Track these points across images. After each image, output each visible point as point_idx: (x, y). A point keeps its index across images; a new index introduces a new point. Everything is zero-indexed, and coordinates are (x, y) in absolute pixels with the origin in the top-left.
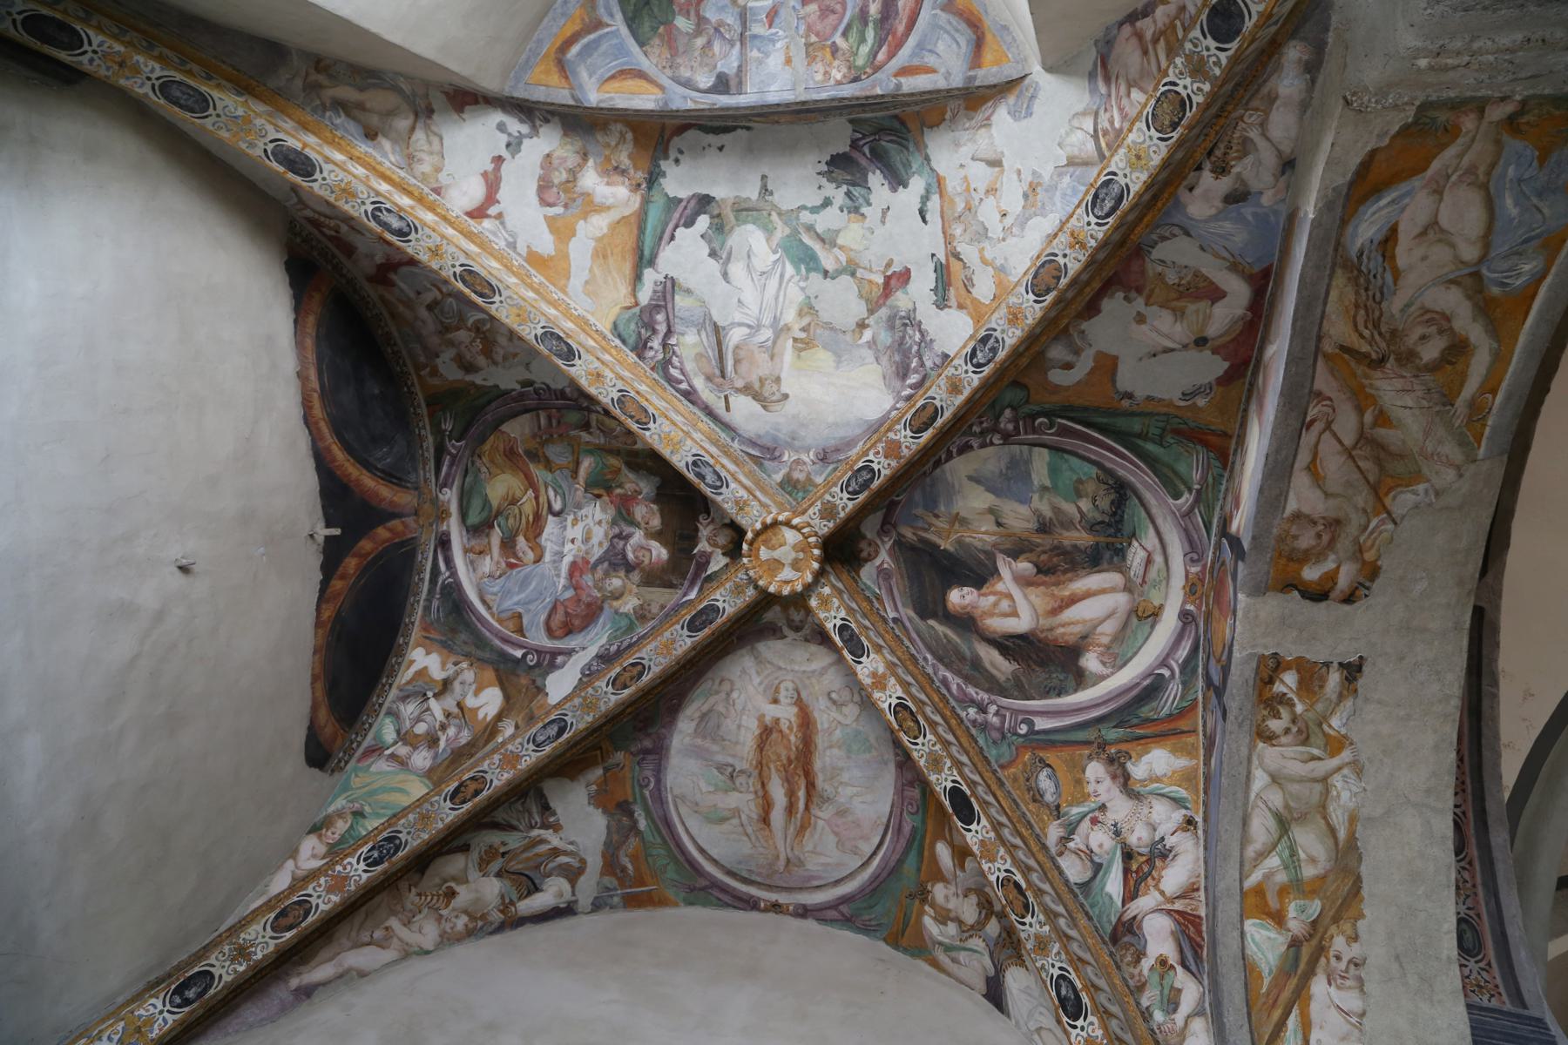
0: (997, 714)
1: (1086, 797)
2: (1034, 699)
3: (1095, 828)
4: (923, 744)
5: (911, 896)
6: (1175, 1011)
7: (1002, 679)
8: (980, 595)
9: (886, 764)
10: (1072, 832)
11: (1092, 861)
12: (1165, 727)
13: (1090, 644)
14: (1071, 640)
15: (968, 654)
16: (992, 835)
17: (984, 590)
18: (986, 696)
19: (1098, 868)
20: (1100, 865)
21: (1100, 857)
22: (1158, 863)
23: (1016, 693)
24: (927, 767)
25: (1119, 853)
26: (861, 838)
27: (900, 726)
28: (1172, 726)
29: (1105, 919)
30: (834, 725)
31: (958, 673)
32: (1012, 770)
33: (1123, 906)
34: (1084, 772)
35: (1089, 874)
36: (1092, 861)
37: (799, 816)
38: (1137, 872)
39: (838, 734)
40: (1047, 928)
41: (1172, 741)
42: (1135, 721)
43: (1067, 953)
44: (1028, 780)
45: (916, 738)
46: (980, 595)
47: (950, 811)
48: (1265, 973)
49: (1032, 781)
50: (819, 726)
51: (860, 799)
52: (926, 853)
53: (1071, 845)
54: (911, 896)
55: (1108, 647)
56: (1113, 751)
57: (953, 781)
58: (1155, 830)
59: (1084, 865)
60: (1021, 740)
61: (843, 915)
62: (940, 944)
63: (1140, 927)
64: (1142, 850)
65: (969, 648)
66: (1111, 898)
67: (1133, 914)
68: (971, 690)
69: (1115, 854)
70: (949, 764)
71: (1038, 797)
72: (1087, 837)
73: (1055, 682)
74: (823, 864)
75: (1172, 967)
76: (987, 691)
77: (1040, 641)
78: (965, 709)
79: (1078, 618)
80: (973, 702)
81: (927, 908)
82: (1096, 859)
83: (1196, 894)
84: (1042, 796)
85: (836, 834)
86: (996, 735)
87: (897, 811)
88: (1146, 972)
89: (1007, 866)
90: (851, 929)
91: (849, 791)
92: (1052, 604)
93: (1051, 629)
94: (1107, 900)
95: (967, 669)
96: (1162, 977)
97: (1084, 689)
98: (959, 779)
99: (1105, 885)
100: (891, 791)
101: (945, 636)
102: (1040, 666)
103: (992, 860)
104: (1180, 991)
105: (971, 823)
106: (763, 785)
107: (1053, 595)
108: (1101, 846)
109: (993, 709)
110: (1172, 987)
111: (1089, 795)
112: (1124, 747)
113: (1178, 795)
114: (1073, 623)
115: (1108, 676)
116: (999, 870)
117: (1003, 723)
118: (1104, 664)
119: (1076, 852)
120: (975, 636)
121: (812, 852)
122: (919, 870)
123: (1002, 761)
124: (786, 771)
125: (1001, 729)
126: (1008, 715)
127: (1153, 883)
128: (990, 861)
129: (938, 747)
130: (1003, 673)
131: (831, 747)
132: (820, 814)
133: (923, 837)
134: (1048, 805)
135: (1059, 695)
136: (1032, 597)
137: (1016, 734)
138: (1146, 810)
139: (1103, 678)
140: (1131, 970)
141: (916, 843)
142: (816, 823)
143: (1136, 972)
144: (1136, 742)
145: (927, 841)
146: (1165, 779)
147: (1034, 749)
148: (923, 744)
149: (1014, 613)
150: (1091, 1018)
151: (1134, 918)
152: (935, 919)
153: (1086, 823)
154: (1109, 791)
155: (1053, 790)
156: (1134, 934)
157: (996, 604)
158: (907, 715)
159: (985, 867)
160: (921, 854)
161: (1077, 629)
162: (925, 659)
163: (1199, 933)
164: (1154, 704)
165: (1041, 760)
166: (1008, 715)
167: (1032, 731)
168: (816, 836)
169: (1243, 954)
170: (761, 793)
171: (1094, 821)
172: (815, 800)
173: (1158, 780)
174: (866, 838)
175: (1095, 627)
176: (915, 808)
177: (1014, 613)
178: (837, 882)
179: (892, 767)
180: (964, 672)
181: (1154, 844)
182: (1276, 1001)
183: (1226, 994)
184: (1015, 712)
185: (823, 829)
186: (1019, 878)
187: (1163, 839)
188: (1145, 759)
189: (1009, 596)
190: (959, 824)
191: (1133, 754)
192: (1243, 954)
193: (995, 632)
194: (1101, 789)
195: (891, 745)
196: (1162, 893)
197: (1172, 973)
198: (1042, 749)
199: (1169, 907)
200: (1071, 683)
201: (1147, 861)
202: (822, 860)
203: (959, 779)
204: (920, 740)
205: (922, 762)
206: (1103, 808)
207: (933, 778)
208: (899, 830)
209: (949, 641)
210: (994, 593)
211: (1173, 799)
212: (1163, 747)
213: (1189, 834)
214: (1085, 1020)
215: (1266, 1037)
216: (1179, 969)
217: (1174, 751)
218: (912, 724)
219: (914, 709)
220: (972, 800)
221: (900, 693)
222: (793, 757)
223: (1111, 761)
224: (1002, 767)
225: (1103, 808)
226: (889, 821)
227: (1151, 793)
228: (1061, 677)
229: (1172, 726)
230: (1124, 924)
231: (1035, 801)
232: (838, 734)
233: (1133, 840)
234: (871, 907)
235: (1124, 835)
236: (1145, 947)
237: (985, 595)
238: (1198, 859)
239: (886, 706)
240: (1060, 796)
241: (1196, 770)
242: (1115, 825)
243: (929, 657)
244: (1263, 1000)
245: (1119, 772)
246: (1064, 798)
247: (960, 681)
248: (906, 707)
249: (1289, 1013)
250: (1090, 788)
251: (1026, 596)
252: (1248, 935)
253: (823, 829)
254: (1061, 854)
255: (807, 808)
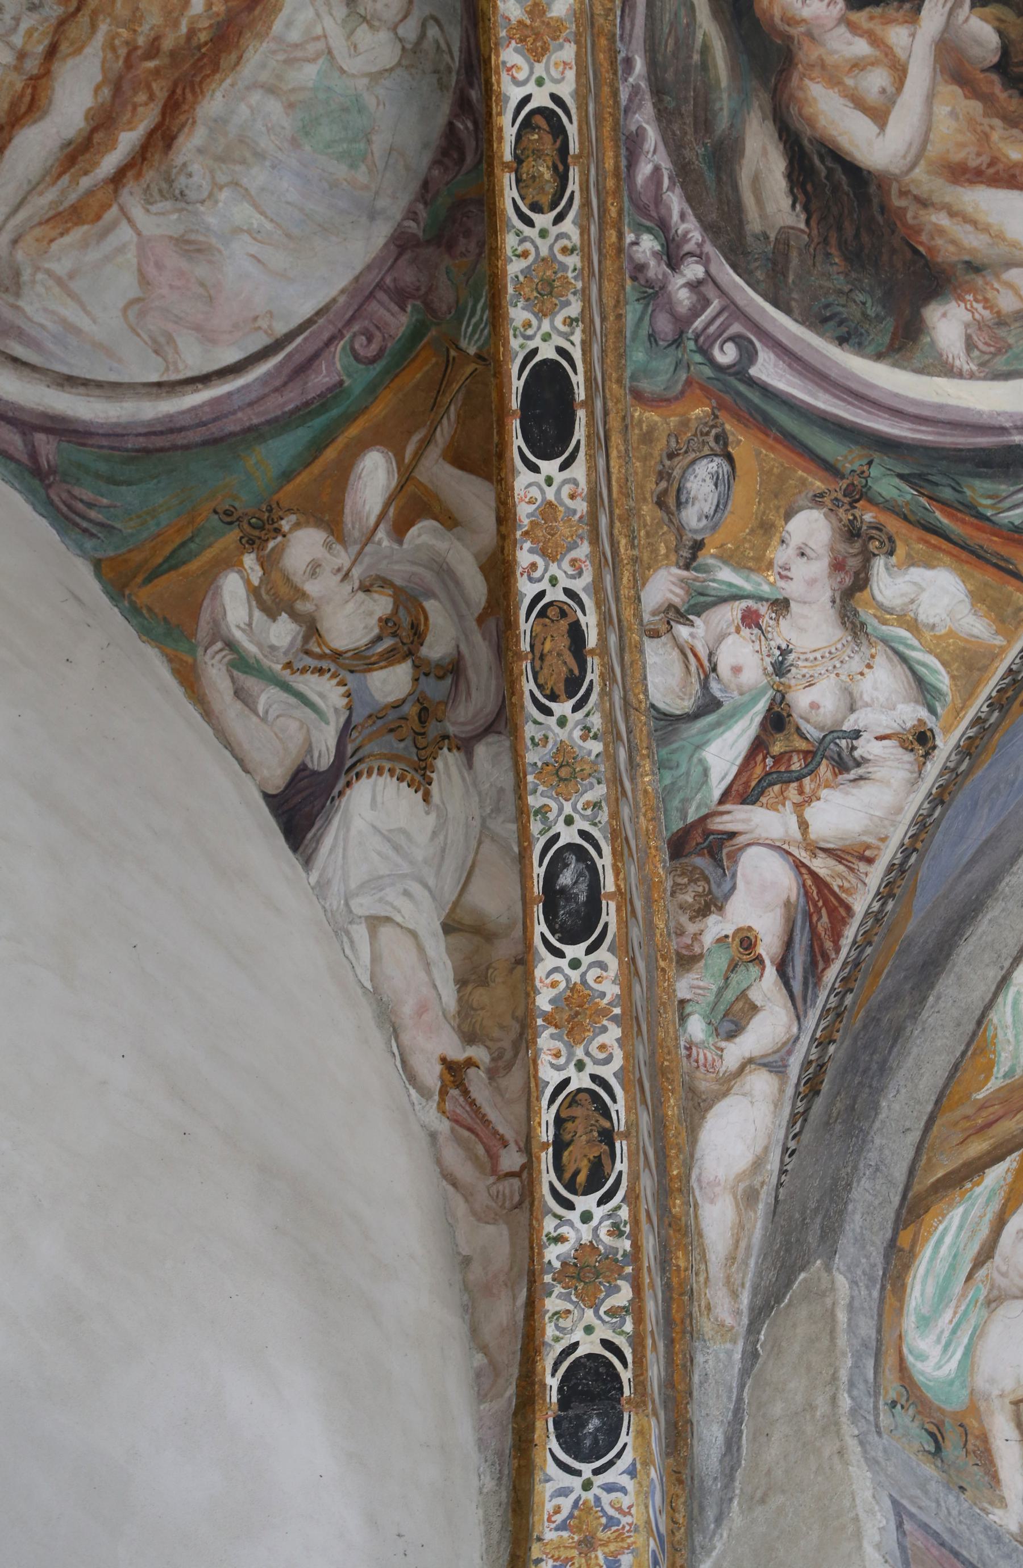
0: (695, 286)
1: (761, 564)
2: (788, 311)
3: (745, 632)
4: (543, 234)
5: (229, 517)
6: (731, 1036)
7: (754, 223)
8: (843, 20)
9: (373, 215)
10: (699, 610)
11: (705, 685)
12: (993, 544)
13: (974, 290)
14: (946, 253)
15: (723, 122)
16: (581, 507)
17: (861, 17)
18: (696, 235)
19: (708, 705)
20: (717, 704)
21: (725, 689)
22: (824, 769)
23: (760, 275)
24: (519, 286)
25: (761, 706)
26: (198, 328)
27: (519, 160)
28: (1006, 551)
29: (676, 803)
30: (312, 48)
31: (674, 146)
32: (652, 416)
33: (724, 799)
34: (788, 516)
35: (684, 705)
36: (705, 685)
37: (86, 182)
38: (777, 759)
39: (309, 73)
40: (596, 747)
41: (988, 576)
42: (947, 493)
43: (615, 815)
44: (671, 456)
45: (536, 208)
46: (843, 20)
47: (515, 404)
48: (1001, 1070)
49: (680, 462)
50: (278, 26)
51: (254, 248)
52: (330, 454)
53: (683, 631)
54: (229, 517)
55: (1001, 321)
56: (868, 517)
57: (561, 351)
58: (852, 710)
59: (685, 684)
60: (708, 371)
61: (33, 455)
62: (231, 645)
63: (734, 857)
64: (805, 727)
65: (734, 114)
66: (706, 772)
67: (730, 827)
68: (675, 202)
69: (754, 700)
70: (574, 309)
71: (671, 502)
72: (722, 637)
73: (852, 312)
74: (64, 322)
75: (759, 960)
76: (709, 228)
77: (883, 209)
78: (639, 229)
79: (992, 219)
80: (662, 227)
81: (249, 560)
82: (715, 687)
83: (862, 867)
84: (679, 504)
85: (144, 280)
86: (664, 325)
87: (324, 329)
88: (708, 939)
89: (578, 585)
90: (29, 494)
91: (242, 213)
92: (969, 155)
93: (924, 203)
94: (696, 772)
95: (696, 153)
96: (733, 967)
97: (895, 365)
98: (577, 354)
99: (707, 742)
100: (342, 280)
101: (706, 49)
102: (846, 259)
103: (549, 554)
104: (754, 1009)
105: (548, 457)
106: (52, 52)
107: (985, 138)
108: (737, 670)
109: (694, 270)
110: (743, 995)
111: (770, 565)
112: (893, 525)
113: (930, 678)
114: (974, 223)
115: (960, 375)
116: (553, 581)
117: (695, 313)
118: (970, 345)
119: (685, 651)
120: (765, 97)
121: (59, 281)
122: (287, 476)
123: (645, 385)
124: (129, 65)
125: (682, 323)
126: (715, 305)
127: (797, 799)
128: (543, 553)
129: (573, 261)
130: (763, 216)
131: (271, 90)
132: (137, 212)
133: (349, 418)
134: (680, 530)
135: (842, 341)
136: (942, 111)
137: (705, 352)
138: (856, 664)
139: (948, 370)
140: (684, 919)
141: (319, 422)
142: (114, 225)
143: (692, 928)
144: (917, 533)
145: (353, 431)
146: (928, 635)
147: (721, 406)
148: (543, 234)
149: (879, 116)
150: (602, 954)
151: (732, 835)
152: (254, 592)
153: (730, 613)
154: (812, 582)
155: (708, 508)
156: (719, 863)
157: (858, 65)
158: (549, 146)
159: (524, 557)
160: (317, 447)
161: (973, 241)
162: (629, 62)
163: (836, 936)
164: (1003, 488)
165: (722, 438)
166: (715, 305)
167: (740, 371)
168: (93, 255)
169: (983, 1015)
170: (32, 66)
171: (750, 619)
172: (149, 175)
173: (913, 626)
174: (207, 336)
175: (1009, 265)
176: (374, 348)
177: (879, 116)
178: (69, 382)
179: (381, 233)
180: (687, 153)
181: (834, 733)
182: (989, 1125)
183: (910, 1062)
184: (733, 309)
185: (121, 250)
186: (590, 621)
187: (857, 734)
188: (917, 573)
189: (900, 71)
190: (518, 441)
191: (901, 550)
192: (983, 1015)
193: (811, 122)
194: (801, 570)
195: (415, 186)
196: (804, 825)
197: (754, 970)
198: (739, 418)
199: (803, 856)
200: (882, 335)
201: (806, 753)
202: (70, 312)
203: (577, 354)
204: (542, 220)
205: (515, 268)
206: (781, 606)
207: (518, 314)
208: (303, 368)
209: (705, 66)
210: (875, 40)
211: (919, 681)
212: (965, 577)
213: (909, 757)
214: (589, 951)
215: (940, 1174)
216: (771, 972)
217: (978, 597)
218: (547, 175)
219: (574, 147)
220: (581, 414)
221: (566, 90)
222: (168, 44)
223: (852, 532)
224: (638, 395)
225: (781, 606)
226: (290, 337)
227: (885, 641)
228: (871, 312)
229: (1006, 551)
230: (707, 833)
231: (661, 503)
232: (309, 73)
233: (801, 700)
234: (112, 481)
235: (790, 679)
236: (727, 897)
237: (853, 28)
238: (899, 810)
239: (516, 94)
240: (714, 528)
241: (994, 655)
242: (785, 652)
243: (639, 65)
244: (968, 1110)
245: (853, 563)
246: (719, 537)
247: (666, 165)
248: (559, 131)
249: (1001, 1158)
250: (781, 555)
251: (930, 98)
252: (1012, 991)
253: (121, 250)
254: (655, 634)
255: (118, 179)
